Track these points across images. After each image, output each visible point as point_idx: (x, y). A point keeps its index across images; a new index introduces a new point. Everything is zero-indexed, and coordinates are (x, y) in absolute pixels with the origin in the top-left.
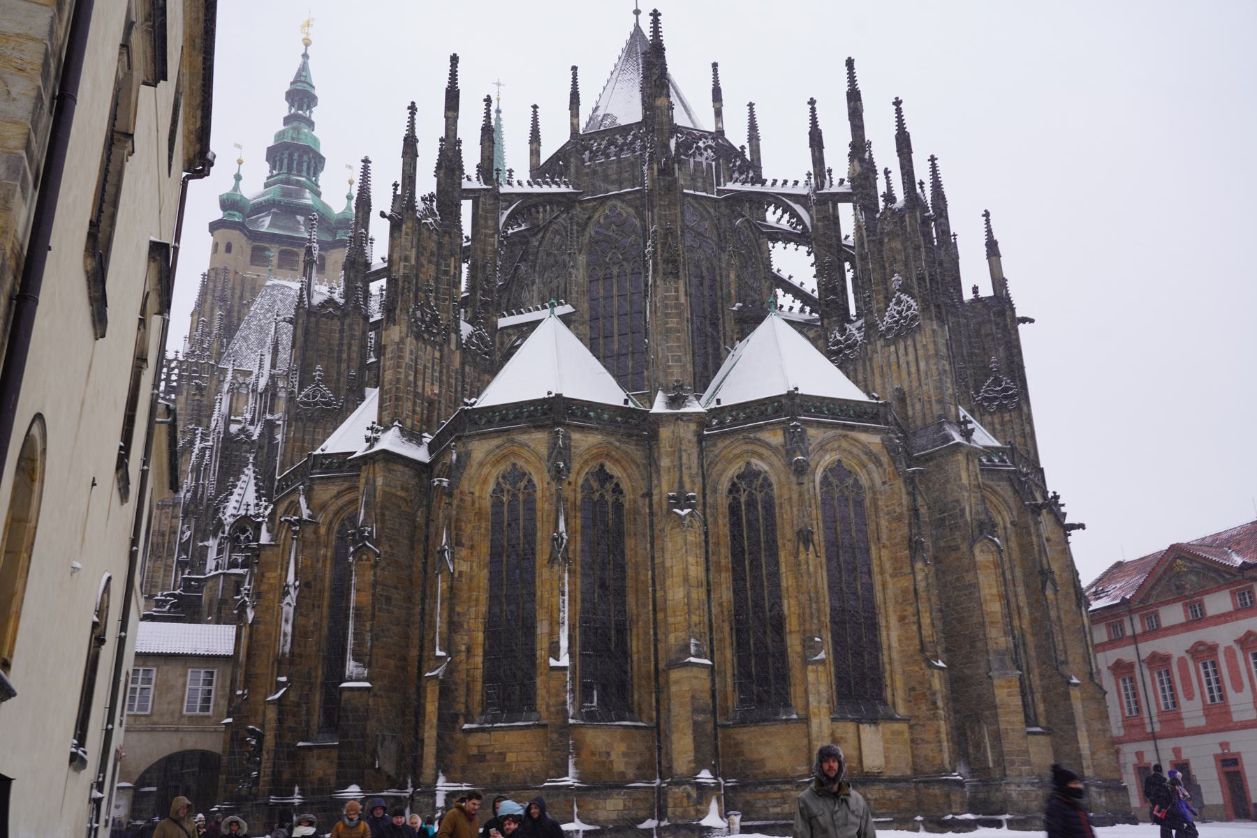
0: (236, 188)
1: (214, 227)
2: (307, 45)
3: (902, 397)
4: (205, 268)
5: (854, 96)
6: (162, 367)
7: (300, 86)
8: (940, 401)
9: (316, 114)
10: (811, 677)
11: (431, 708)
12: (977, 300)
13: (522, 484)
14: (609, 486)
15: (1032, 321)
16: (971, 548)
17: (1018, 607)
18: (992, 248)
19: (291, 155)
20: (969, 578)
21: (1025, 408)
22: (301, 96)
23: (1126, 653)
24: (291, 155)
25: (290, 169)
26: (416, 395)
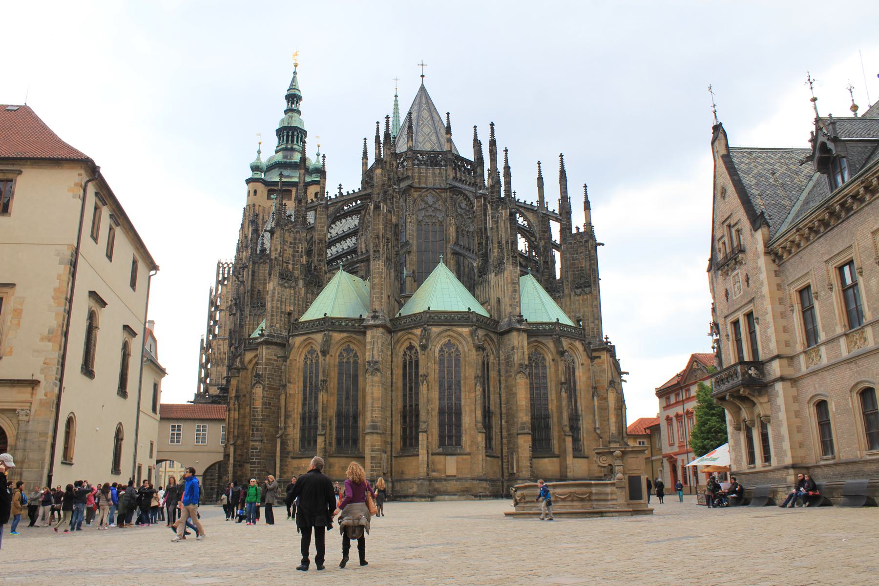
0: (258, 159)
1: (248, 181)
2: (296, 66)
3: (499, 301)
4: (245, 205)
5: (493, 143)
7: (292, 92)
8: (511, 305)
9: (302, 106)
10: (420, 438)
11: (278, 449)
12: (578, 233)
13: (314, 356)
14: (351, 355)
15: (603, 245)
16: (516, 375)
17: (552, 400)
18: (587, 206)
19: (288, 133)
20: (514, 389)
21: (594, 292)
22: (293, 98)
23: (679, 410)
24: (288, 133)
25: (287, 141)
26: (282, 313)
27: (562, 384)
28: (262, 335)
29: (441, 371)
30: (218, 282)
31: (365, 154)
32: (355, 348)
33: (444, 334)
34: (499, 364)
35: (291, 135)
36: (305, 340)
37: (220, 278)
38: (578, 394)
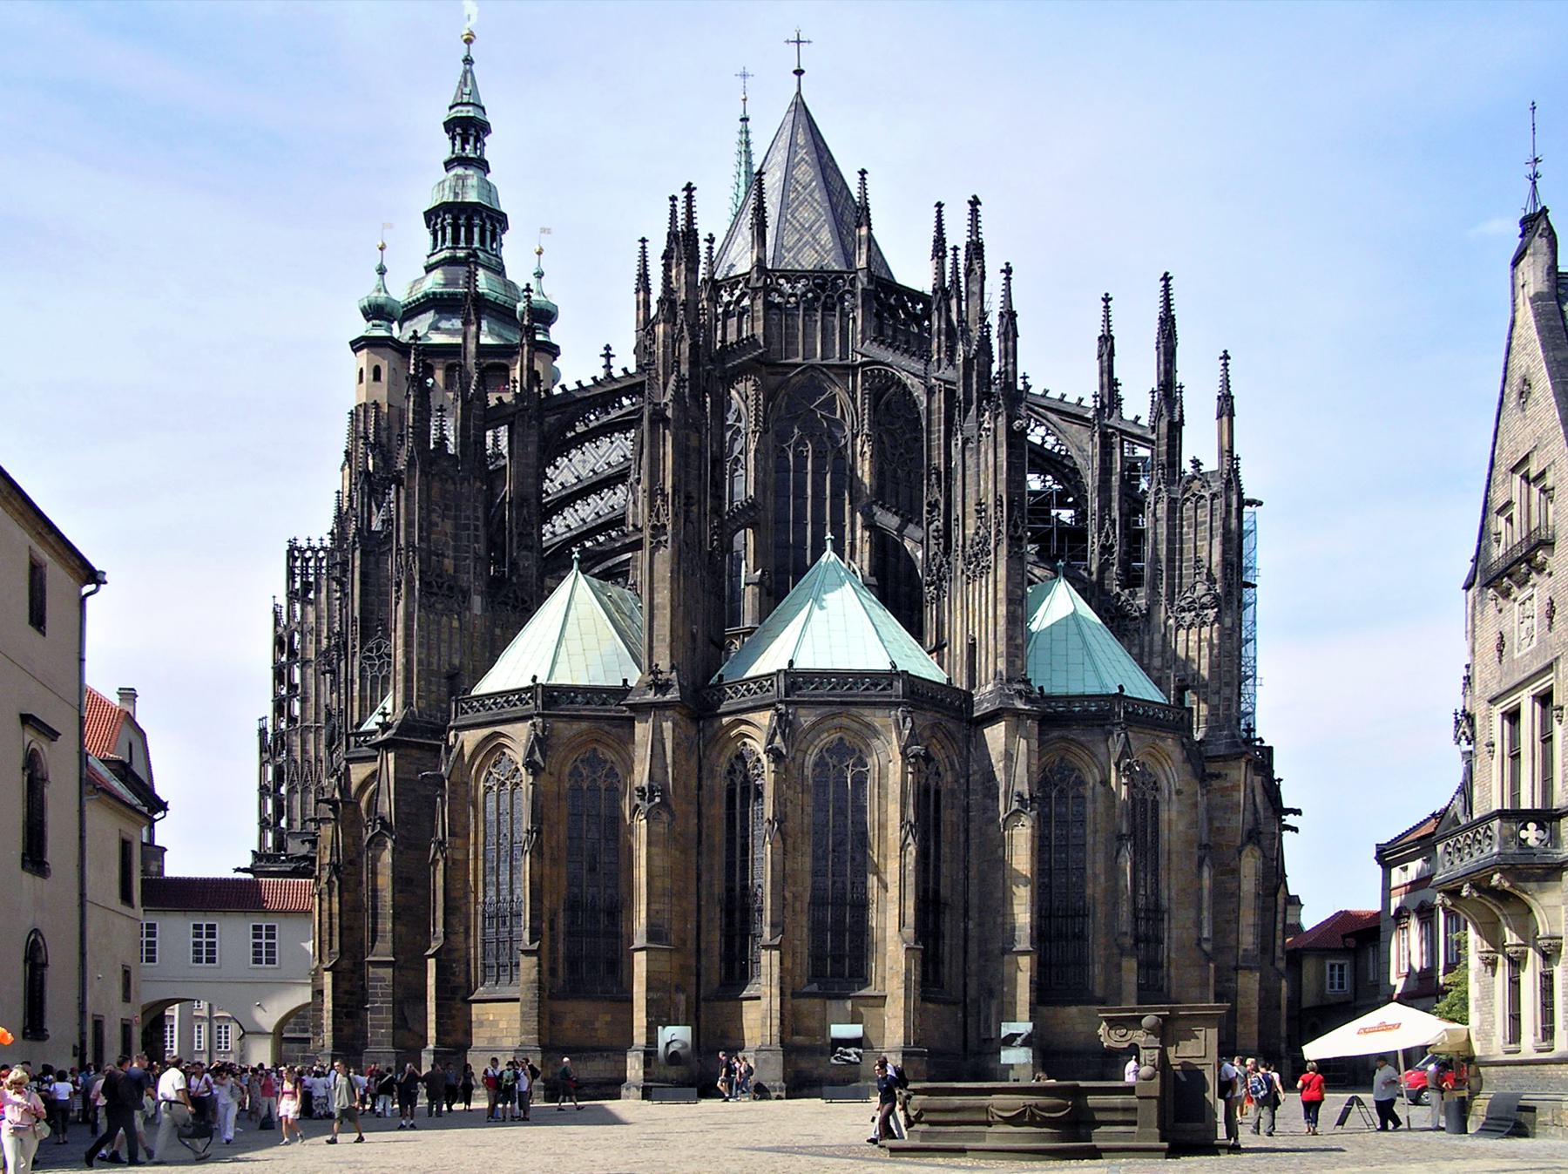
6: (296, 559)
17: (1095, 876)
27: (1120, 837)
28: (385, 727)
29: (820, 807)
30: (292, 596)
31: (643, 278)
32: (610, 756)
33: (829, 723)
34: (967, 793)
35: (469, 225)
36: (488, 739)
37: (298, 586)
38: (1163, 862)
